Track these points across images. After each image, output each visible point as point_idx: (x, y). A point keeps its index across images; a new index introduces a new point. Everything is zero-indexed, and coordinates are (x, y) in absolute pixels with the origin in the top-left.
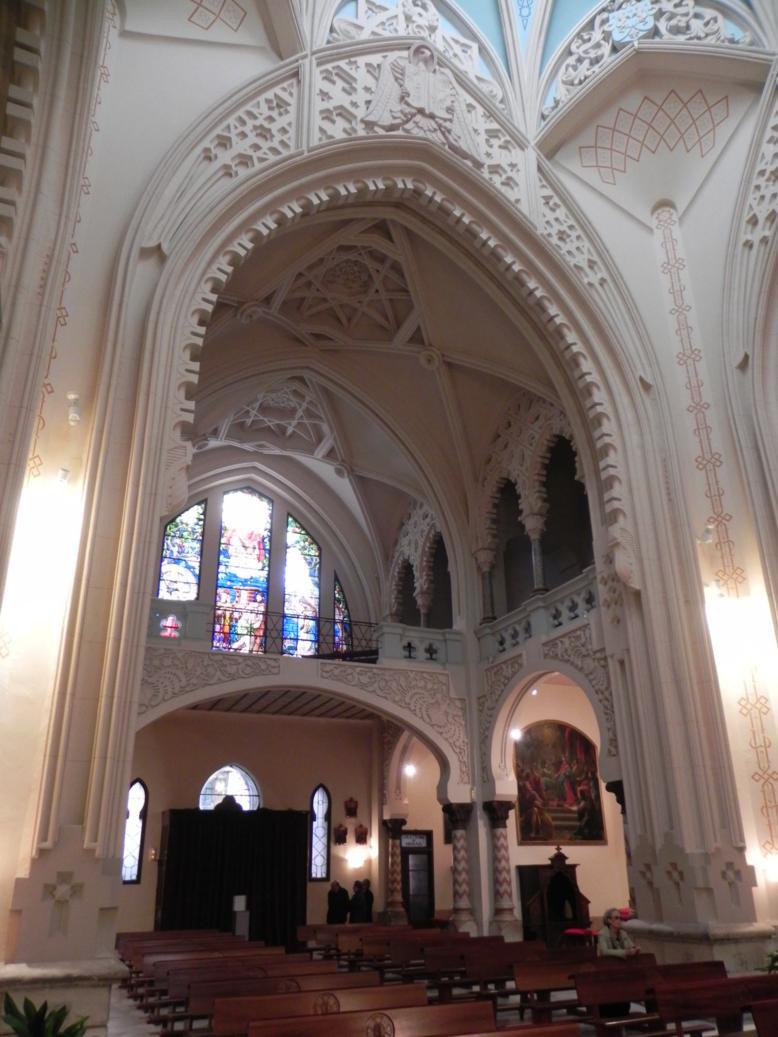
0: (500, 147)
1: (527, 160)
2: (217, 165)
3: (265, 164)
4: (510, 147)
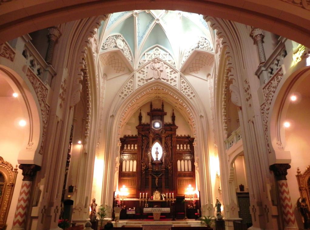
0: (174, 73)
2: (121, 97)
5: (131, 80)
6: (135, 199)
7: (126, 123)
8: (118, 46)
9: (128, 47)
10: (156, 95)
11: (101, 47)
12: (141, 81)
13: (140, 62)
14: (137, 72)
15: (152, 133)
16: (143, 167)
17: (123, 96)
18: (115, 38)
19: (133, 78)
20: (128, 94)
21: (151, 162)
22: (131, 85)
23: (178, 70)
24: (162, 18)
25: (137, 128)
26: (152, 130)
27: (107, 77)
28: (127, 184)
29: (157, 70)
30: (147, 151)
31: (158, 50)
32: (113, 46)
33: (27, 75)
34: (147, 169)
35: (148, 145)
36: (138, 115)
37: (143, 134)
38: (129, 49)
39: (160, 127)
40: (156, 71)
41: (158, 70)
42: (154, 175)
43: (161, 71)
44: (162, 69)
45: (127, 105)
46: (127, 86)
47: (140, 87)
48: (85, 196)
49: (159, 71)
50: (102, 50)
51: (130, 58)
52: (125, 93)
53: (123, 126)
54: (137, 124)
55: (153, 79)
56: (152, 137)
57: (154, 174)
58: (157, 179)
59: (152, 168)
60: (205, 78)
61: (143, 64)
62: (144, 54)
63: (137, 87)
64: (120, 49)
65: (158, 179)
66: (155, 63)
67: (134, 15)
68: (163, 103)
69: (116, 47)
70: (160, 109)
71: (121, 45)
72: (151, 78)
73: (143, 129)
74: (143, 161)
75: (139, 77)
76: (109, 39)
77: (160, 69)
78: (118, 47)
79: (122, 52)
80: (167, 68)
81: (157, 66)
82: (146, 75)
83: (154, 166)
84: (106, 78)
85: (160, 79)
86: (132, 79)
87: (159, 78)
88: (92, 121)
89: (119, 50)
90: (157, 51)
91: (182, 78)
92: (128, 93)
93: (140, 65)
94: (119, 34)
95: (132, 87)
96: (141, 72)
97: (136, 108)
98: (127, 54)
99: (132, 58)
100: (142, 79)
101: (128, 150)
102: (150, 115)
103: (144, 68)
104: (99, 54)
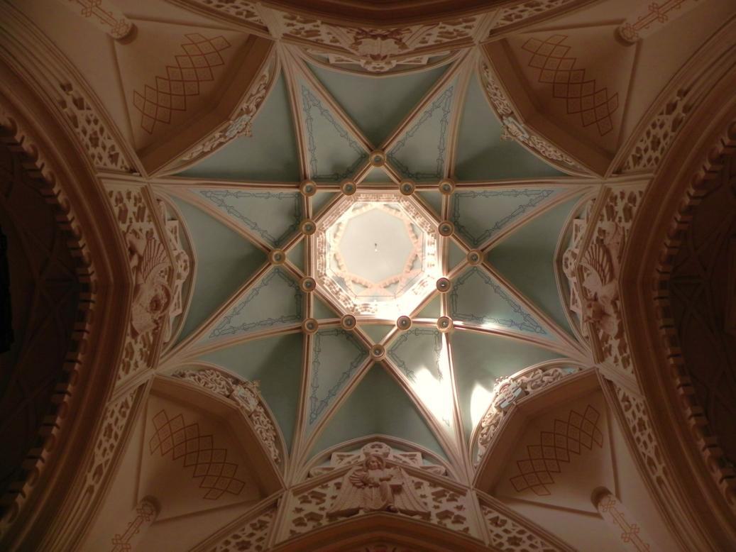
0: (448, 500)
1: (469, 502)
4: (456, 498)
23: (467, 485)
24: (391, 352)
29: (376, 485)
44: (399, 483)
49: (389, 489)
60: (589, 507)
80: (418, 486)
81: (375, 475)
82: (332, 505)
91: (488, 509)
96: (310, 498)
99: (281, 454)
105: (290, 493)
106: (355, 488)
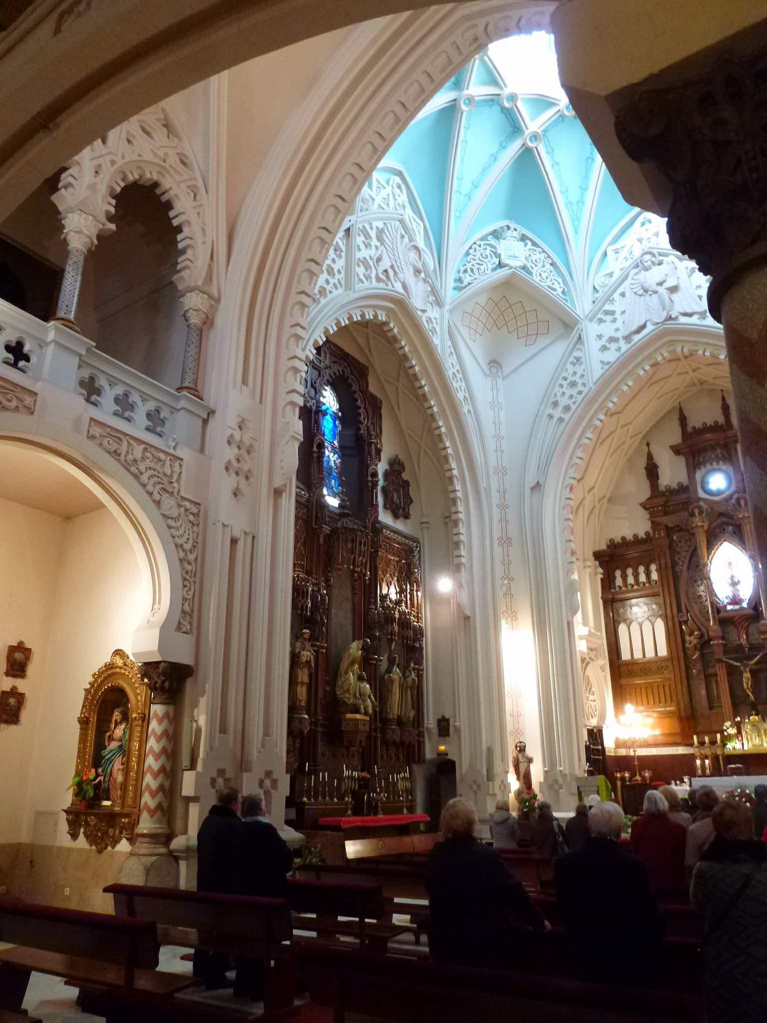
2: (555, 420)
3: (577, 404)
5: (577, 354)
6: (681, 750)
7: (606, 500)
8: (507, 262)
9: (544, 251)
10: (688, 377)
11: (451, 284)
12: (609, 349)
13: (597, 287)
14: (591, 320)
15: (701, 513)
16: (687, 638)
17: (558, 413)
18: (493, 241)
19: (581, 347)
20: (574, 403)
21: (714, 618)
22: (580, 370)
25: (644, 506)
26: (702, 503)
27: (501, 367)
28: (645, 702)
29: (656, 292)
30: (696, 581)
31: (650, 222)
32: (490, 267)
33: (92, 437)
34: (704, 644)
35: (694, 559)
36: (642, 462)
37: (670, 525)
38: (549, 257)
39: (730, 484)
40: (655, 297)
41: (662, 290)
42: (731, 662)
43: (674, 289)
45: (579, 439)
46: (565, 379)
47: (606, 367)
48: (484, 747)
50: (455, 292)
51: (556, 286)
52: (564, 401)
53: (596, 511)
54: (645, 492)
55: (650, 327)
56: (702, 526)
57: (731, 659)
58: (747, 675)
59: (723, 638)
61: (607, 288)
62: (605, 254)
63: (597, 371)
64: (516, 268)
65: (751, 671)
66: (646, 269)
67: (530, 145)
68: (724, 399)
69: (501, 265)
70: (716, 422)
71: (517, 255)
72: (643, 327)
73: (669, 507)
74: (685, 618)
75: (600, 337)
76: (471, 251)
77: (667, 285)
78: (505, 266)
79: (523, 273)
83: (732, 632)
84: (500, 373)
85: (676, 318)
86: (578, 349)
87: (670, 318)
88: (468, 515)
89: (513, 275)
90: (647, 225)
92: (573, 400)
93: (597, 295)
94: (504, 223)
95: (582, 376)
96: (604, 318)
97: (629, 441)
98: (544, 275)
100: (612, 340)
101: (629, 587)
102: (684, 454)
103: (612, 301)
104: (447, 308)
105: (588, 322)
106: (638, 297)
